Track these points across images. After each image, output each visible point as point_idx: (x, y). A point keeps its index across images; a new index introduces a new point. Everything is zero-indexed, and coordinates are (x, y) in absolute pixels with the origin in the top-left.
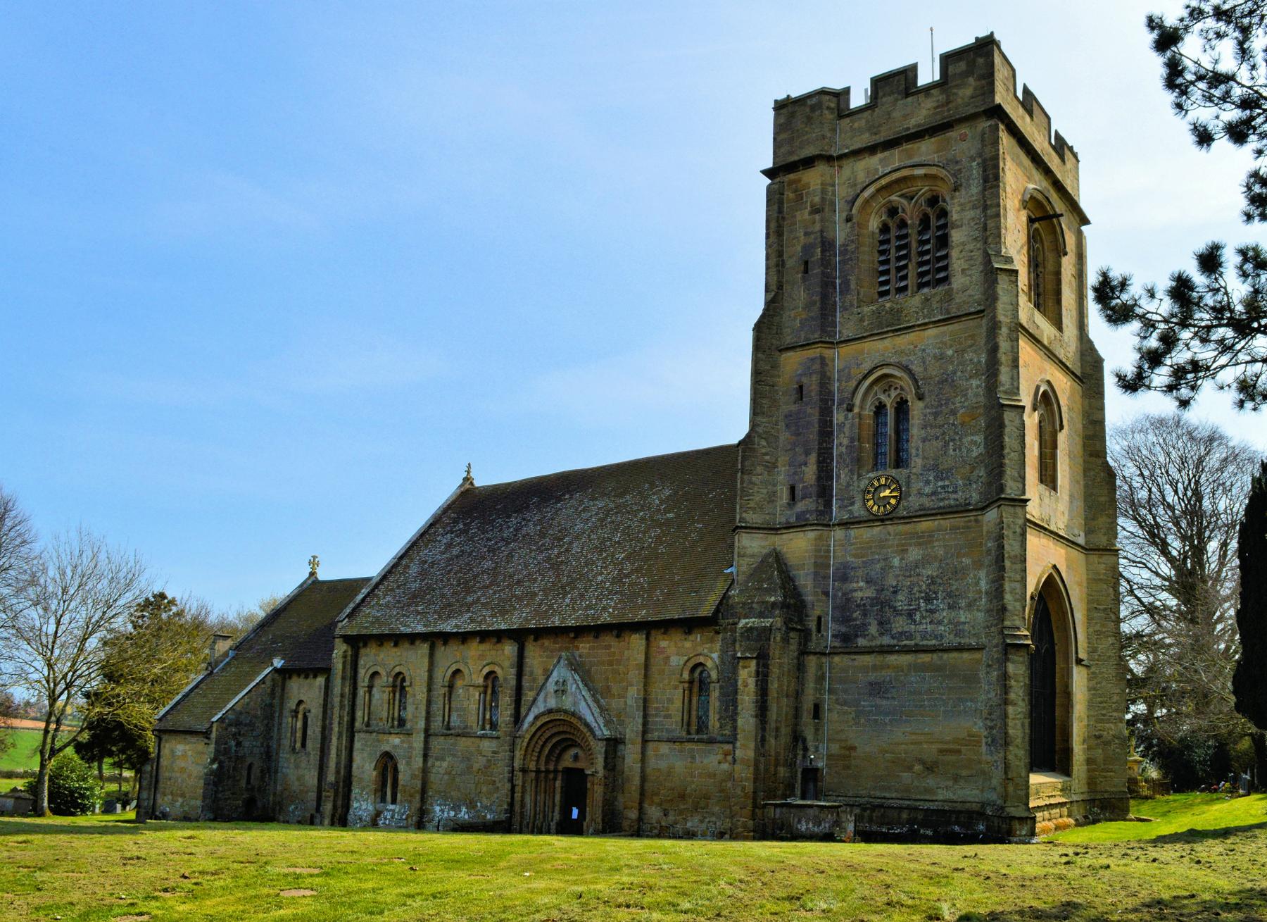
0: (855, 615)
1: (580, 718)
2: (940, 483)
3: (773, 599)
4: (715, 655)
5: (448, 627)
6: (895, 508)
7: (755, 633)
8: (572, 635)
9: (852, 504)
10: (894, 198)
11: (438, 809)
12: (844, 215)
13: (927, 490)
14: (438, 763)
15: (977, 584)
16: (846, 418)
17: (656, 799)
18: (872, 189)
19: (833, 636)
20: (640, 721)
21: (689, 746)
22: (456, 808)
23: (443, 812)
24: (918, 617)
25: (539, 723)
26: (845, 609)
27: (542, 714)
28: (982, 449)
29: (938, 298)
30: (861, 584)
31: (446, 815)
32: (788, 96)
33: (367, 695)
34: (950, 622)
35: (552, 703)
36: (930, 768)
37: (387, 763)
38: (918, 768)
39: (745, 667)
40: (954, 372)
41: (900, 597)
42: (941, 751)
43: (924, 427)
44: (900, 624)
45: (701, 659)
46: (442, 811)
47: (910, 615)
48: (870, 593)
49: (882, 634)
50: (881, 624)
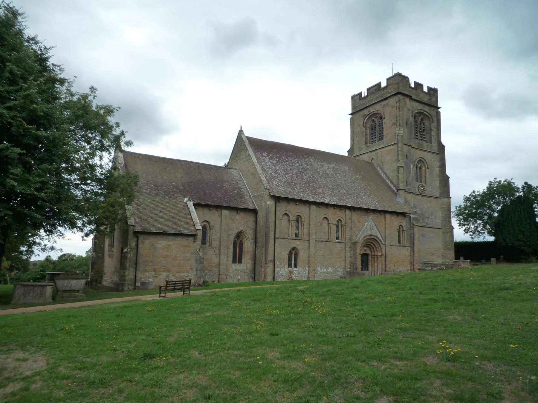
1: (378, 238)
9: (416, 189)
10: (417, 115)
11: (319, 269)
13: (430, 190)
14: (318, 252)
21: (400, 247)
22: (327, 268)
23: (321, 270)
24: (430, 219)
27: (367, 236)
31: (323, 270)
35: (369, 232)
36: (433, 254)
38: (431, 254)
39: (416, 227)
41: (426, 214)
44: (426, 221)
48: (420, 212)
50: (423, 220)
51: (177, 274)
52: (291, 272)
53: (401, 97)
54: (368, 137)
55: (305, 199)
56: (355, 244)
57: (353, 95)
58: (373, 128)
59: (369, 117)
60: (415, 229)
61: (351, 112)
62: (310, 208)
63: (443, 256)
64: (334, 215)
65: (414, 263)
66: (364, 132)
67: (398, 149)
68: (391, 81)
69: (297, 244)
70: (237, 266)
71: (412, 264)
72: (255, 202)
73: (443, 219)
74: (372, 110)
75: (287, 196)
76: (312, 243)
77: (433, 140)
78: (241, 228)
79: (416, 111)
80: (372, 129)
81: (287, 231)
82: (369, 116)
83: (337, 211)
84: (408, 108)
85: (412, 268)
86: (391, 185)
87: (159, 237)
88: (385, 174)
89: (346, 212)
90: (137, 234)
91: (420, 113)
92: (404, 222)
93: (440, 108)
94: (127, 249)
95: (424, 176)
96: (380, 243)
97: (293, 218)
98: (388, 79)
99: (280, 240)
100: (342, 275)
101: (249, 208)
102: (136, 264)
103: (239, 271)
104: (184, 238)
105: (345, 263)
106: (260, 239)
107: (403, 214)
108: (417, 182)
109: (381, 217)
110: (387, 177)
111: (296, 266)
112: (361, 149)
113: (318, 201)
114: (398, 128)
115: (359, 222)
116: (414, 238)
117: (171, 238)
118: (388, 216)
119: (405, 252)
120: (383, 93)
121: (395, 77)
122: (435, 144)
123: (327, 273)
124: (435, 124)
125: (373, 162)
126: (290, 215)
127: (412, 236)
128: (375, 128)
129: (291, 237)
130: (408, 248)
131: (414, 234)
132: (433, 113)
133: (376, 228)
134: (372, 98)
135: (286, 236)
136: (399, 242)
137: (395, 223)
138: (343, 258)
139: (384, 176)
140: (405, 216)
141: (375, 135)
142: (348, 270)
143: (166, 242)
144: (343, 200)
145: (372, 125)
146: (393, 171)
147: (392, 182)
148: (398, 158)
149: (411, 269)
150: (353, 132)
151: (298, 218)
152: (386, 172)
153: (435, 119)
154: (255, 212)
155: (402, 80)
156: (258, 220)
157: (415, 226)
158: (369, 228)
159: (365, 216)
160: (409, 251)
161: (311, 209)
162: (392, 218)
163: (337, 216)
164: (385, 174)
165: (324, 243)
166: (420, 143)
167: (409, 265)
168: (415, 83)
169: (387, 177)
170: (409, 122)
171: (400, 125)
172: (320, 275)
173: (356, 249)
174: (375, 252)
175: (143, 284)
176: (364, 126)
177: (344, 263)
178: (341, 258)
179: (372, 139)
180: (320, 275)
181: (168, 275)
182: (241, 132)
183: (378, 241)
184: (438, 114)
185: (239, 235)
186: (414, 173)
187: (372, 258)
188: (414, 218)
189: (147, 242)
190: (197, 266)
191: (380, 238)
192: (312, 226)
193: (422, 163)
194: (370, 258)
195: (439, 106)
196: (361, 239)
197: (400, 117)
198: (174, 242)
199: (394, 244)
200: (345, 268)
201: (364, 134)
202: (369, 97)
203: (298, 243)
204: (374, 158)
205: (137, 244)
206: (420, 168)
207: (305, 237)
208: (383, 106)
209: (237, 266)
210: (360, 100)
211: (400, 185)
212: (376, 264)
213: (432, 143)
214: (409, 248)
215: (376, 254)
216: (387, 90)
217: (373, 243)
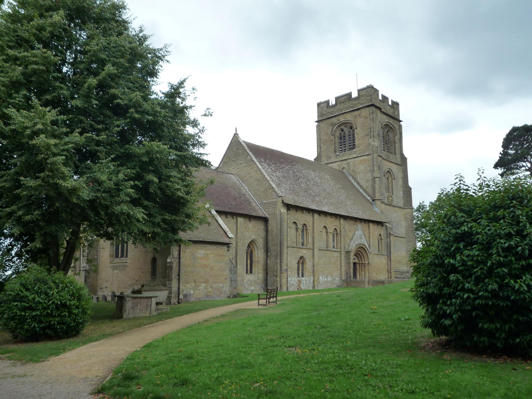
1: (366, 247)
11: (321, 278)
13: (396, 201)
22: (327, 277)
37: (302, 260)
46: (323, 278)
51: (215, 286)
52: (300, 282)
53: (375, 109)
54: (337, 145)
55: (310, 207)
56: (348, 253)
57: (319, 102)
58: (342, 138)
59: (338, 126)
60: (392, 238)
61: (317, 120)
62: (313, 217)
64: (332, 224)
65: (391, 271)
66: (332, 140)
67: (373, 159)
68: (363, 93)
69: (304, 252)
70: (249, 276)
71: (389, 272)
72: (264, 210)
74: (342, 119)
75: (297, 205)
76: (316, 251)
77: (397, 152)
78: (253, 237)
79: (384, 124)
80: (341, 138)
81: (295, 240)
82: (339, 124)
85: (389, 276)
86: (365, 194)
87: (198, 246)
88: (358, 183)
89: (340, 220)
93: (402, 121)
94: (171, 259)
95: (391, 187)
96: (367, 251)
98: (359, 91)
100: (339, 284)
101: (261, 216)
103: (252, 281)
104: (219, 247)
105: (341, 272)
106: (273, 249)
107: (380, 223)
109: (366, 226)
110: (361, 186)
111: (303, 276)
112: (329, 157)
113: (320, 210)
114: (372, 139)
115: (350, 231)
116: (390, 247)
117: (208, 246)
118: (371, 225)
119: (384, 260)
120: (354, 103)
121: (368, 89)
122: (398, 156)
123: (327, 282)
124: (397, 137)
125: (345, 171)
126: (298, 223)
127: (389, 244)
128: (345, 137)
129: (298, 246)
131: (390, 243)
132: (396, 126)
134: (342, 107)
135: (295, 245)
137: (376, 232)
138: (339, 267)
139: (357, 186)
140: (383, 226)
141: (345, 144)
142: (344, 278)
143: (204, 251)
144: (337, 209)
145: (341, 134)
146: (367, 181)
147: (366, 192)
148: (374, 169)
149: (388, 277)
150: (320, 140)
152: (360, 181)
153: (398, 133)
154: (265, 220)
155: (374, 92)
156: (270, 228)
157: (391, 235)
158: (359, 237)
159: (354, 224)
160: (386, 259)
161: (315, 217)
162: (374, 227)
164: (358, 183)
165: (324, 252)
167: (387, 273)
168: (382, 95)
169: (361, 186)
170: (380, 134)
171: (374, 136)
172: (322, 285)
173: (350, 258)
174: (362, 261)
175: (185, 296)
176: (332, 135)
177: (339, 271)
179: (341, 148)
180: (322, 285)
181: (206, 286)
182: (236, 135)
184: (400, 126)
185: (251, 244)
187: (359, 266)
189: (188, 251)
190: (231, 276)
191: (368, 247)
192: (316, 235)
194: (358, 267)
195: (401, 119)
197: (373, 128)
198: (211, 251)
200: (341, 277)
201: (333, 142)
202: (338, 106)
203: (305, 251)
204: (346, 167)
207: (310, 246)
208: (354, 116)
209: (249, 277)
210: (328, 108)
211: (377, 195)
212: (363, 273)
213: (397, 155)
215: (363, 262)
216: (359, 101)
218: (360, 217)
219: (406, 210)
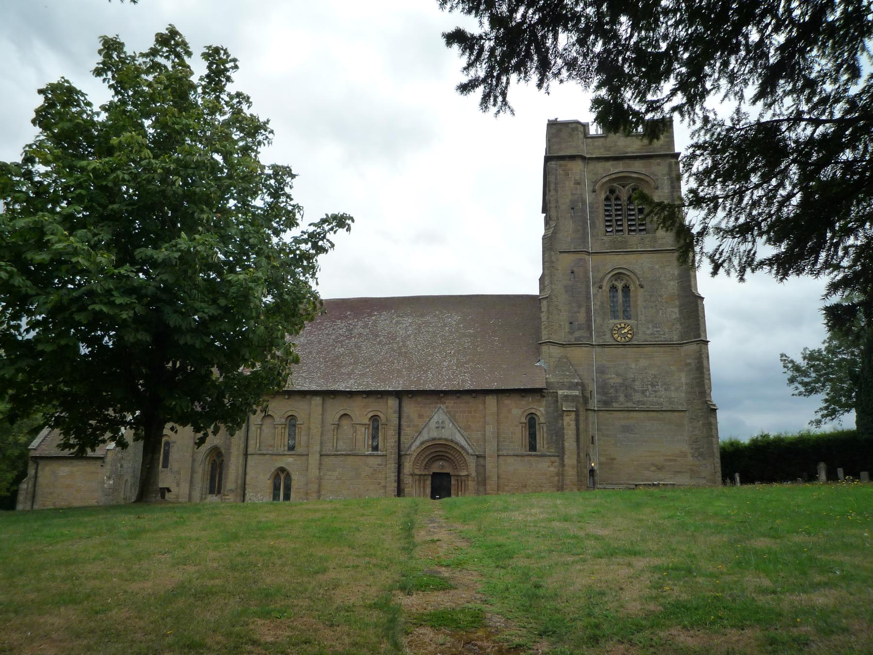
0: (610, 391)
1: (457, 444)
2: (655, 329)
3: (576, 381)
4: (542, 409)
5: (342, 387)
6: (631, 339)
7: (570, 398)
8: (442, 395)
9: (604, 335)
10: (615, 185)
12: (591, 188)
13: (649, 332)
14: (330, 473)
15: (680, 379)
16: (598, 291)
17: (507, 488)
18: (607, 179)
19: (598, 401)
20: (496, 444)
21: (527, 459)
24: (647, 393)
25: (424, 447)
26: (603, 388)
27: (427, 441)
28: (677, 315)
29: (648, 239)
30: (613, 376)
32: (556, 119)
33: (259, 430)
34: (666, 397)
35: (435, 434)
36: (660, 468)
38: (653, 468)
39: (567, 416)
40: (660, 277)
42: (666, 460)
43: (645, 301)
44: (637, 397)
45: (533, 411)
47: (643, 392)
48: (619, 380)
49: (627, 402)
50: (626, 396)
63: (692, 470)
73: (689, 390)
83: (371, 400)
84: (575, 180)
90: (37, 459)
91: (622, 180)
92: (541, 409)
97: (279, 419)
99: (255, 457)
102: (34, 497)
108: (615, 317)
111: (287, 497)
115: (420, 416)
118: (491, 401)
130: (553, 459)
133: (451, 424)
136: (533, 447)
151: (292, 420)
157: (565, 413)
159: (437, 403)
163: (369, 410)
165: (342, 458)
166: (619, 239)
178: (379, 483)
183: (458, 448)
186: (599, 303)
188: (566, 396)
189: (47, 469)
191: (463, 443)
193: (627, 278)
194: (453, 482)
196: (413, 448)
199: (511, 453)
203: (290, 460)
205: (36, 473)
206: (626, 289)
211: (543, 333)
214: (556, 459)
217: (447, 452)
218: (444, 388)
219: (686, 347)
